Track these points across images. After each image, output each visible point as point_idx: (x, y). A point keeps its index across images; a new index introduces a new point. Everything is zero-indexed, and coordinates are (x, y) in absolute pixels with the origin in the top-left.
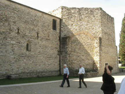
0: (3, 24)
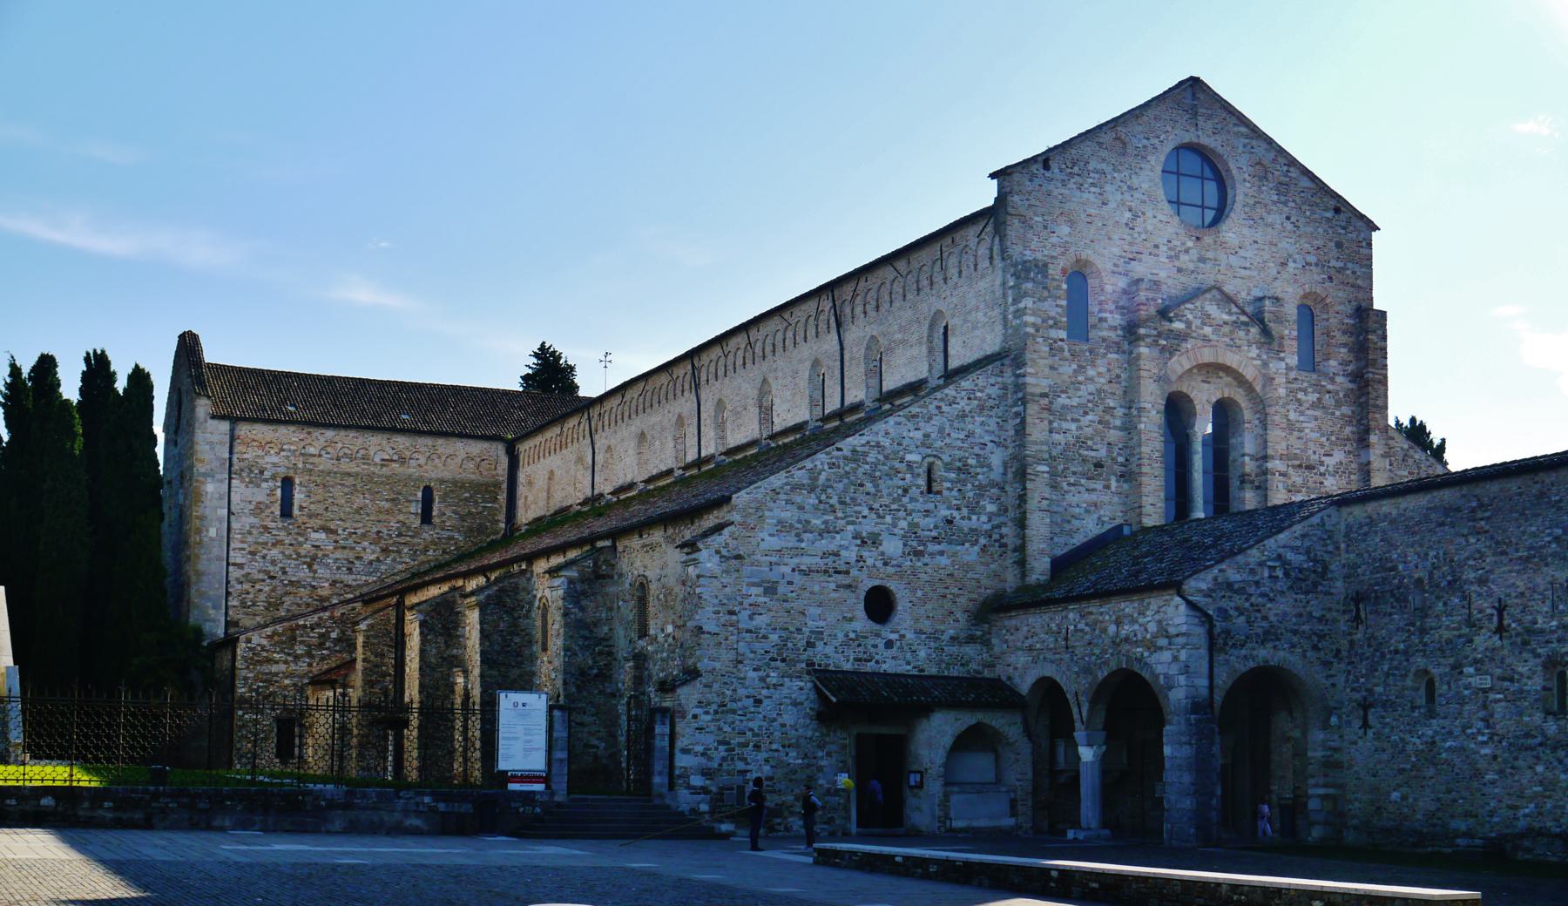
0: (1445, 604)
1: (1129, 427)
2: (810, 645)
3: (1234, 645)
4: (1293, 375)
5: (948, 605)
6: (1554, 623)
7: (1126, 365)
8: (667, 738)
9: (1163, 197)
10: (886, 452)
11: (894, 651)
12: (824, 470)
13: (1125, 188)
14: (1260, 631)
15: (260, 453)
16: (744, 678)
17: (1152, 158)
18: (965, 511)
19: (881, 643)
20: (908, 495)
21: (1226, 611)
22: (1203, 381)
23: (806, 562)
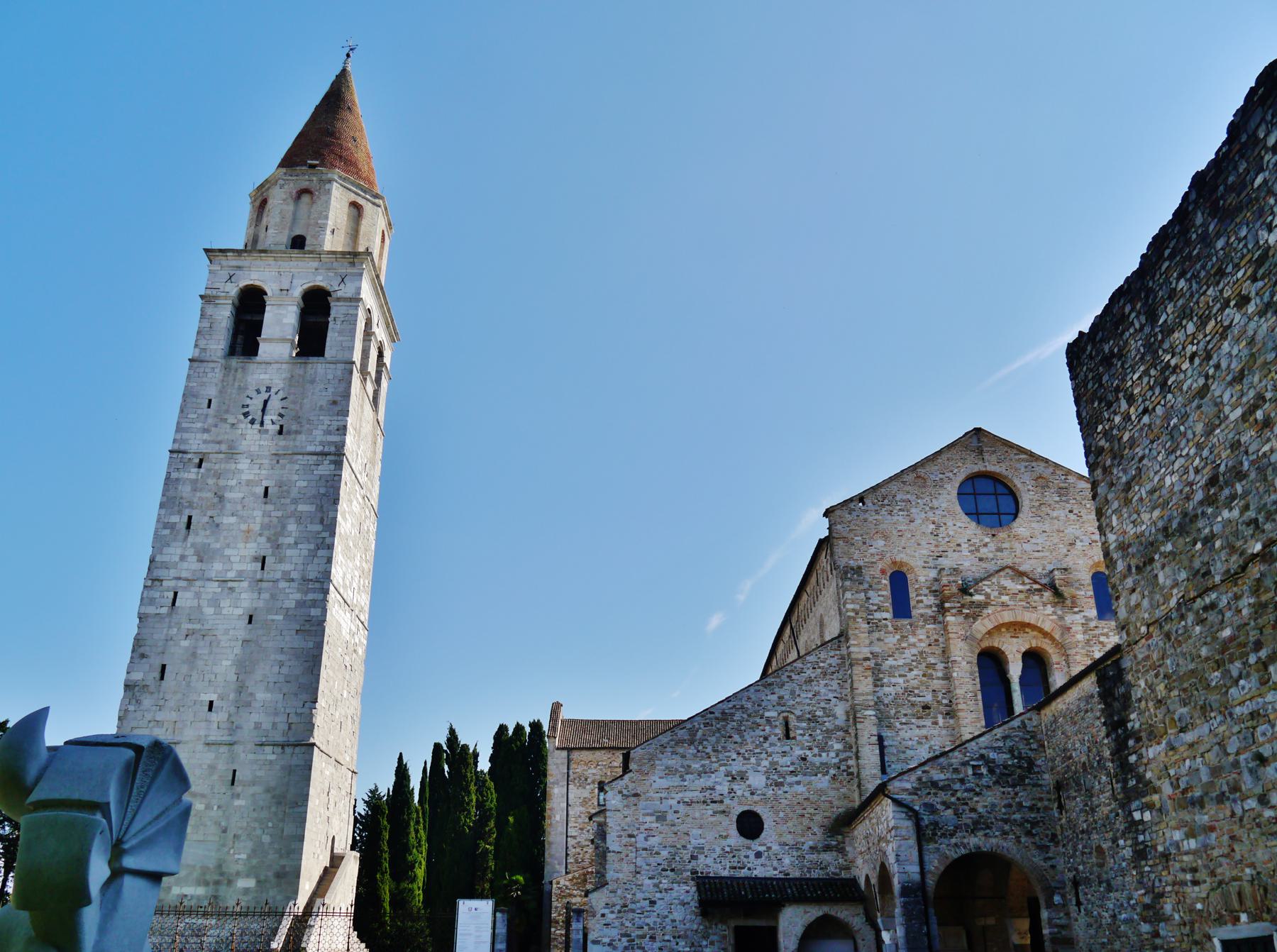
0: (1099, 783)
1: (947, 677)
2: (693, 857)
3: (944, 835)
4: (1092, 624)
5: (806, 822)
7: (942, 632)
8: (581, 933)
9: (961, 511)
10: (749, 712)
11: (762, 860)
12: (700, 728)
13: (928, 508)
14: (969, 821)
15: (585, 768)
16: (642, 885)
17: (948, 486)
18: (816, 750)
19: (752, 854)
20: (768, 742)
21: (932, 805)
22: (1011, 637)
23: (688, 796)
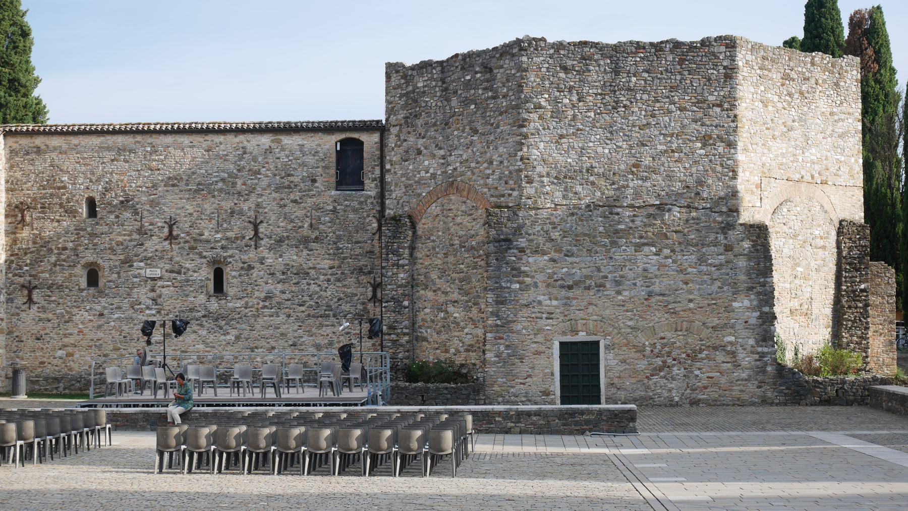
0: (117, 217)
6: (219, 236)
